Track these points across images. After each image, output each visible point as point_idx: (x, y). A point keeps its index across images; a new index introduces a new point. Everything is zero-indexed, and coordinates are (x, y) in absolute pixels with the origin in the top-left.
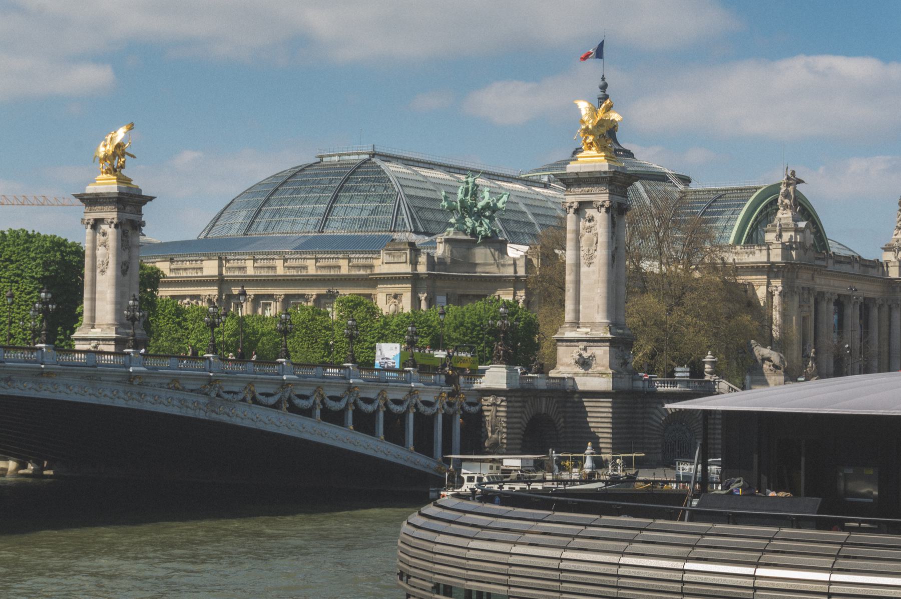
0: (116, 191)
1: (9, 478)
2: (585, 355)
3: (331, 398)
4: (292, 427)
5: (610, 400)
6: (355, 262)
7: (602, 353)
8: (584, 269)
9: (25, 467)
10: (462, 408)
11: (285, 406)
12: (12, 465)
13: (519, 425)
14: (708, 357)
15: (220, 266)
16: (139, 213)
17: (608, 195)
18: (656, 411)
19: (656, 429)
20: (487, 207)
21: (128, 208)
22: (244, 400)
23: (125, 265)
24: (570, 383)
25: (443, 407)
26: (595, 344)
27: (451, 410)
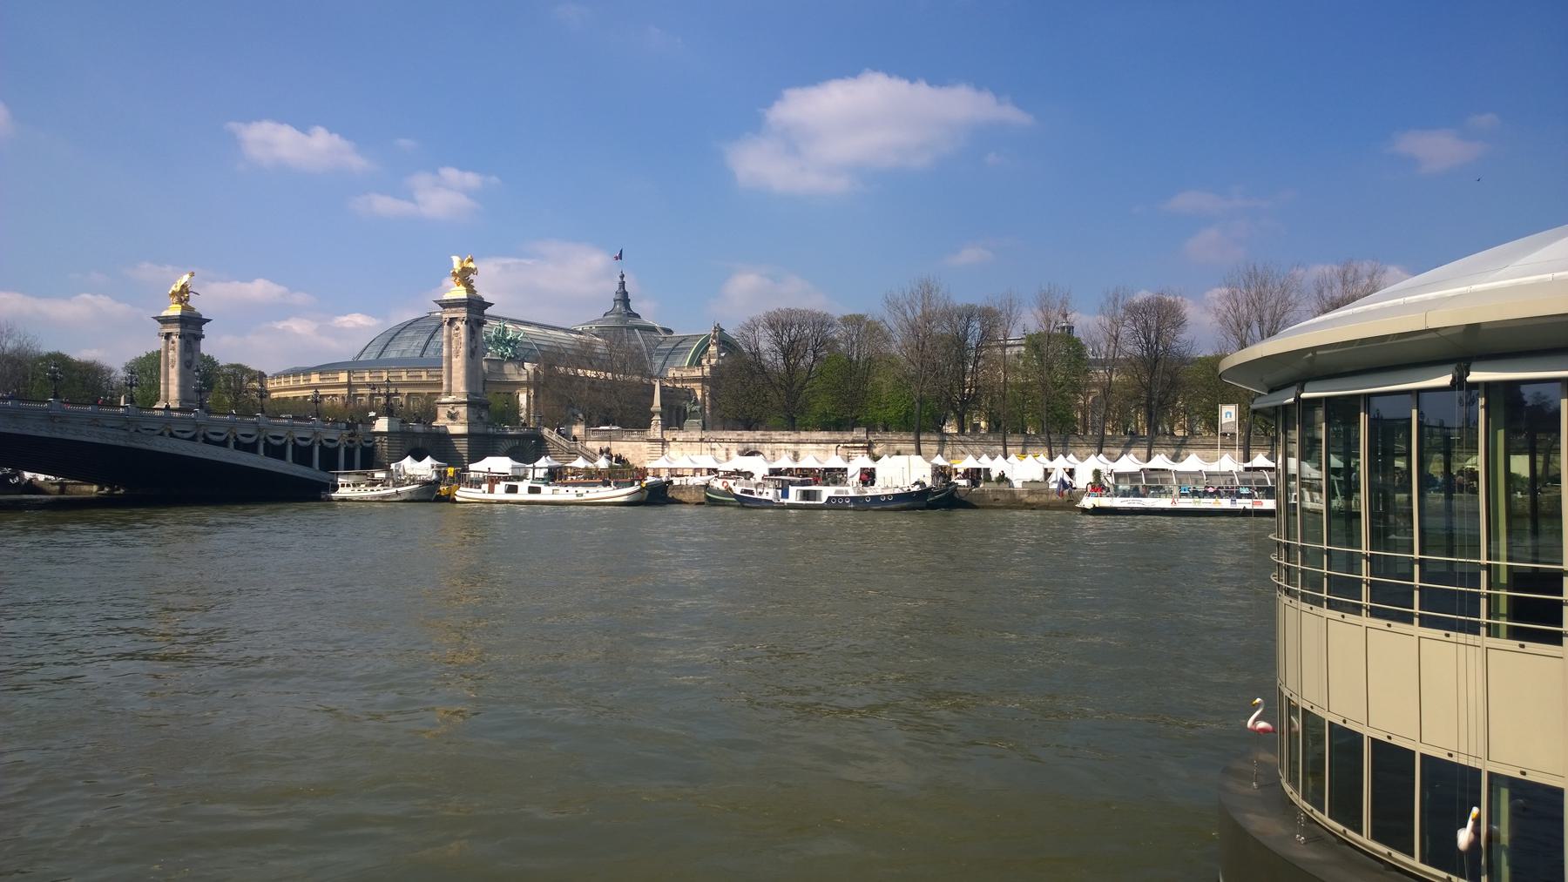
0: (179, 314)
1: (93, 495)
2: (453, 412)
3: (243, 435)
6: (433, 373)
7: (462, 410)
8: (454, 359)
9: (103, 489)
10: (361, 444)
11: (201, 439)
12: (95, 488)
15: (349, 377)
20: (511, 340)
22: (162, 434)
24: (443, 429)
27: (351, 446)
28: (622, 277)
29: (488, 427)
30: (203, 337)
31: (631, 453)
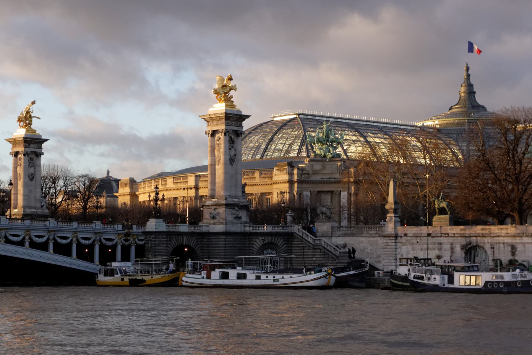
2: (215, 212)
3: (36, 236)
4: (7, 251)
5: (224, 237)
8: (217, 167)
10: (136, 243)
13: (165, 251)
14: (289, 213)
16: (40, 148)
17: (225, 126)
18: (256, 243)
19: (256, 253)
21: (32, 145)
23: (31, 175)
25: (121, 242)
26: (219, 207)
27: (127, 243)
28: (468, 69)
29: (245, 226)
30: (43, 154)
31: (370, 248)
